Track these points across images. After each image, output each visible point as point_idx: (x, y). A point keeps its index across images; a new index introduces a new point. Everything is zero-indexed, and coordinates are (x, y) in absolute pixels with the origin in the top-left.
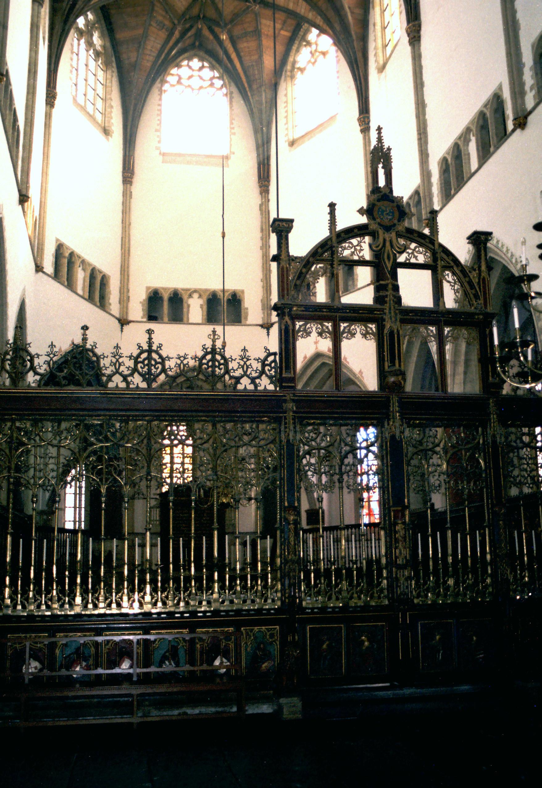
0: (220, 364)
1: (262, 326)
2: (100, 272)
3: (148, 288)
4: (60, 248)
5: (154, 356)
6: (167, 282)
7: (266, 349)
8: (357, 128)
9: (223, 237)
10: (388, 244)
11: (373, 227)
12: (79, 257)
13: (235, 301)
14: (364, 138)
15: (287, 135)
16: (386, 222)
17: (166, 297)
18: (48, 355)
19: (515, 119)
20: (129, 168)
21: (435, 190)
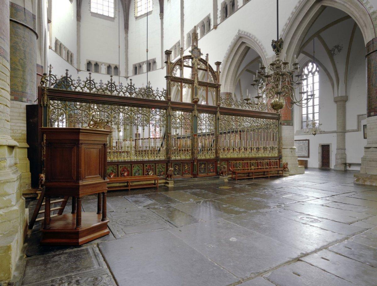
2: (70, 52)
3: (87, 60)
4: (57, 41)
5: (132, 87)
6: (94, 59)
7: (163, 89)
8: (159, 17)
9: (147, 52)
10: (196, 62)
11: (192, 56)
12: (63, 46)
13: (116, 68)
15: (135, 15)
17: (93, 64)
18: (100, 84)
19: (214, 26)
20: (79, 16)
21: (185, 43)
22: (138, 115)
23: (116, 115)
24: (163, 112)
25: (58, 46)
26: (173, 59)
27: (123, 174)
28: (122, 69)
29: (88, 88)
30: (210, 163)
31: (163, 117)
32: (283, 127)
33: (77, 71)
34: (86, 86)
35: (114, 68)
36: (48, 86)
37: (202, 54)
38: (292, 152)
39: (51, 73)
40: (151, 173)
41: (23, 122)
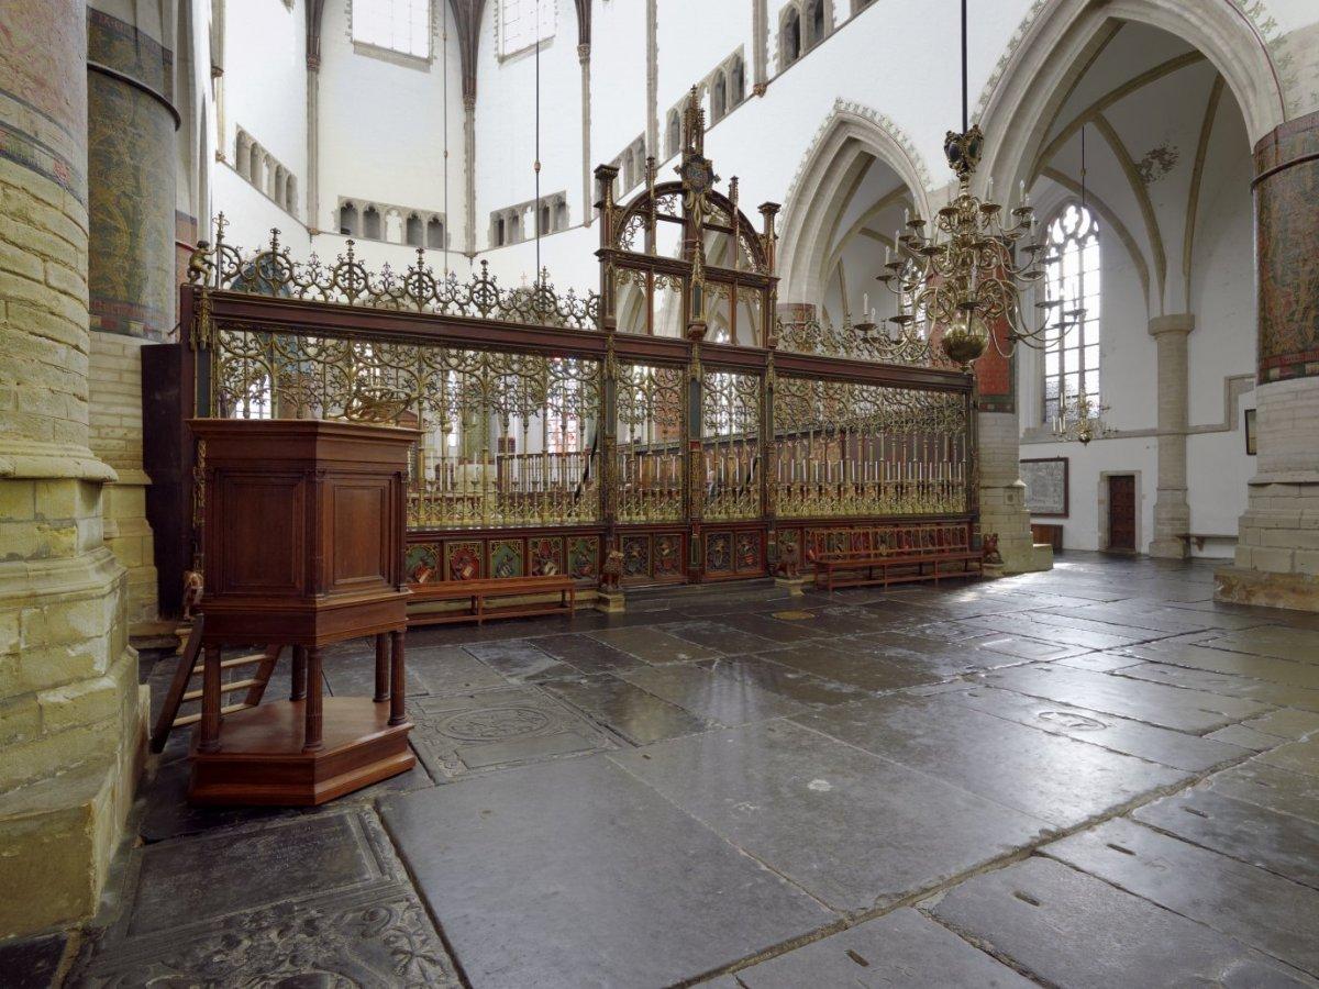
0: (491, 295)
1: (465, 254)
2: (286, 171)
3: (340, 198)
4: (241, 135)
5: (489, 287)
6: (364, 194)
8: (576, 58)
9: (538, 170)
10: (697, 204)
11: (686, 186)
12: (263, 151)
13: (436, 224)
14: (584, 69)
15: (497, 49)
16: (697, 183)
17: (361, 210)
19: (756, 86)
21: (662, 140)
22: (508, 378)
23: (434, 377)
24: (589, 367)
25: (248, 153)
26: (621, 193)
27: (458, 570)
28: (455, 228)
29: (344, 291)
30: (745, 535)
31: (591, 385)
32: (983, 415)
33: (307, 235)
34: (336, 283)
35: (430, 223)
36: (212, 283)
37: (717, 179)
38: (1010, 498)
39: (224, 241)
40: (551, 569)
41: (130, 400)
